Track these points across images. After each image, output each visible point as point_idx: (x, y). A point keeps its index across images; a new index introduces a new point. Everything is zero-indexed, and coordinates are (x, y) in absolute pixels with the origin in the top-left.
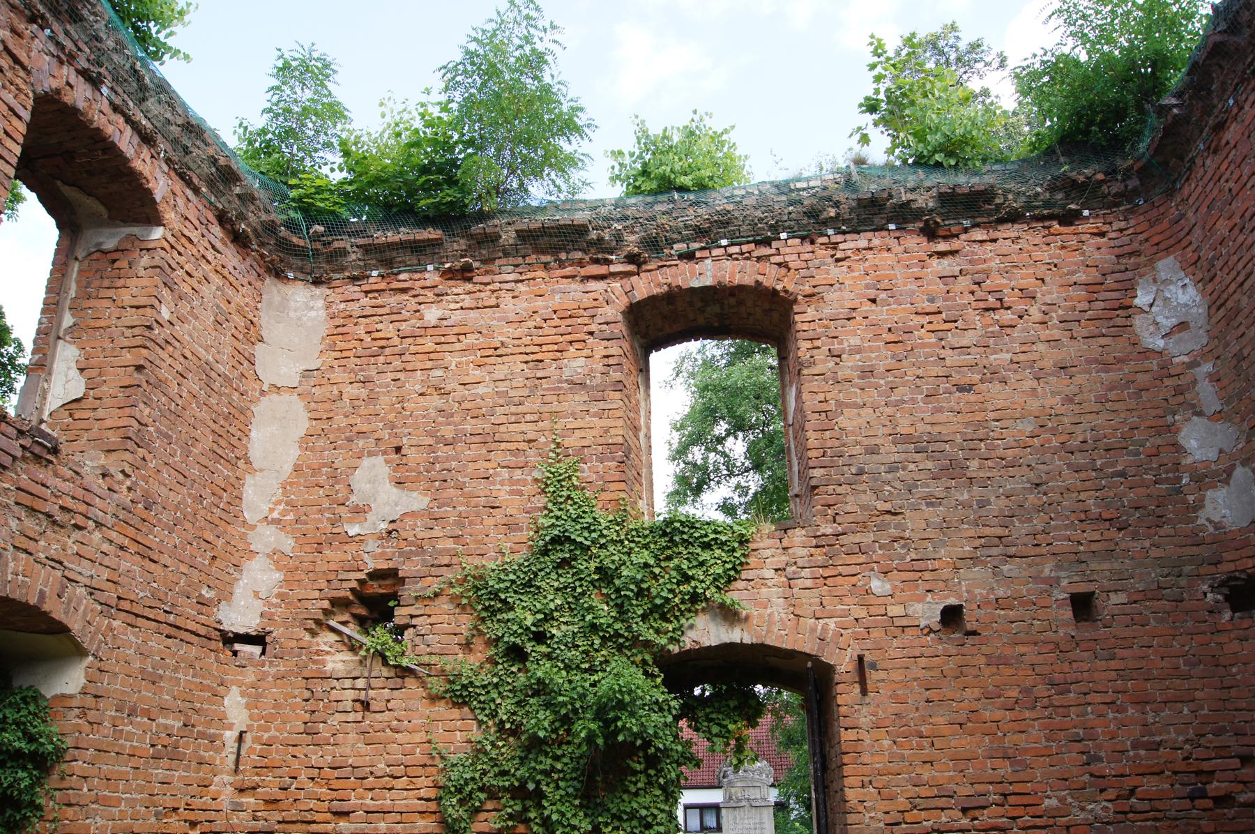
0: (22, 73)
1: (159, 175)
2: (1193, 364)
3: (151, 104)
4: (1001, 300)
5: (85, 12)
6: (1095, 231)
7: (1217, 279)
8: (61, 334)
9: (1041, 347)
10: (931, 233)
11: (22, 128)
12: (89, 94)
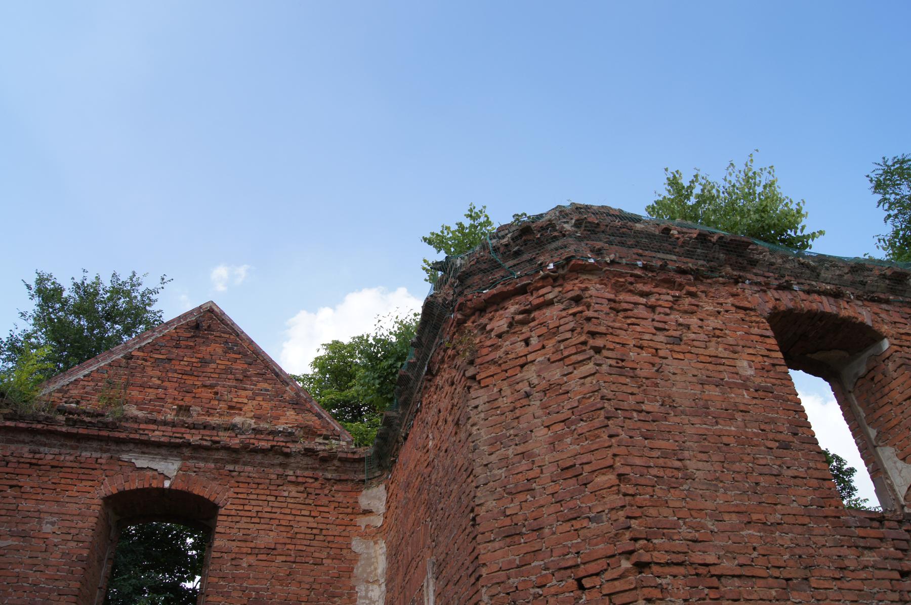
0: (752, 313)
1: (860, 310)
3: (824, 274)
5: (756, 257)
8: (875, 443)
11: (773, 341)
12: (790, 296)
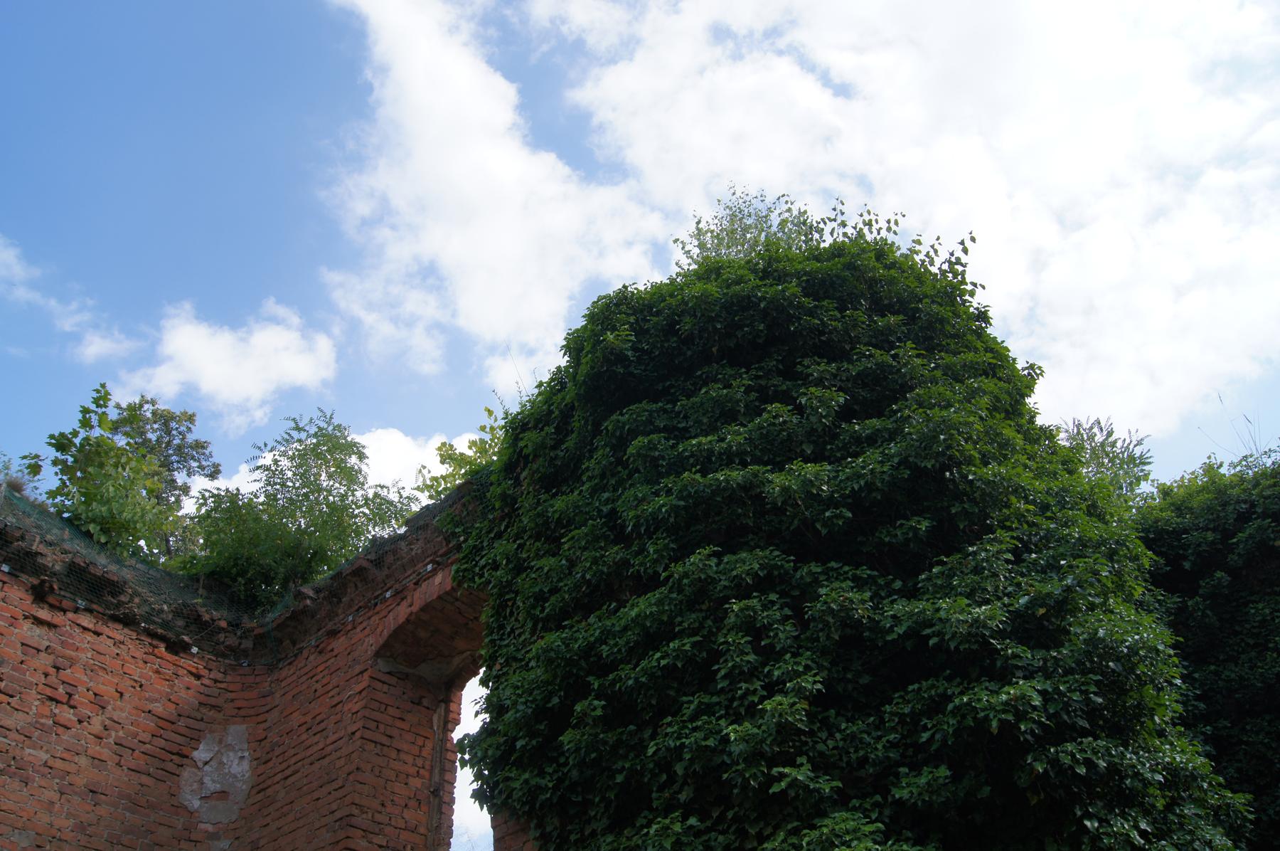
2: (214, 836)
4: (70, 695)
6: (194, 671)
7: (270, 764)
9: (83, 761)
10: (40, 594)
